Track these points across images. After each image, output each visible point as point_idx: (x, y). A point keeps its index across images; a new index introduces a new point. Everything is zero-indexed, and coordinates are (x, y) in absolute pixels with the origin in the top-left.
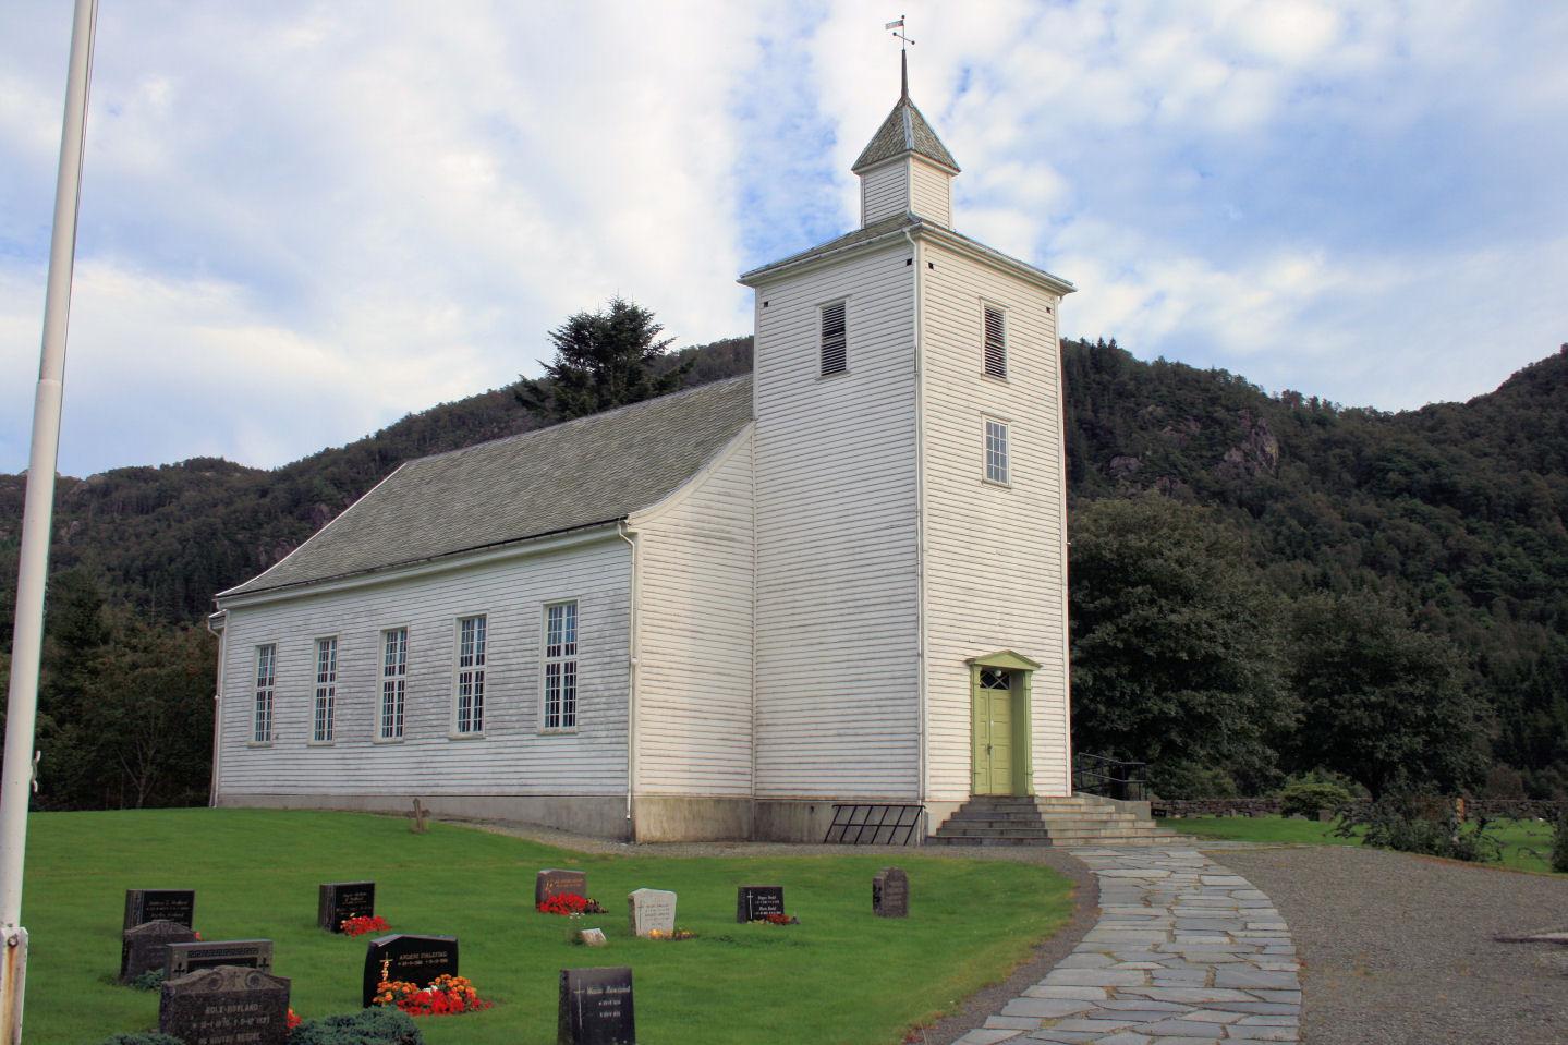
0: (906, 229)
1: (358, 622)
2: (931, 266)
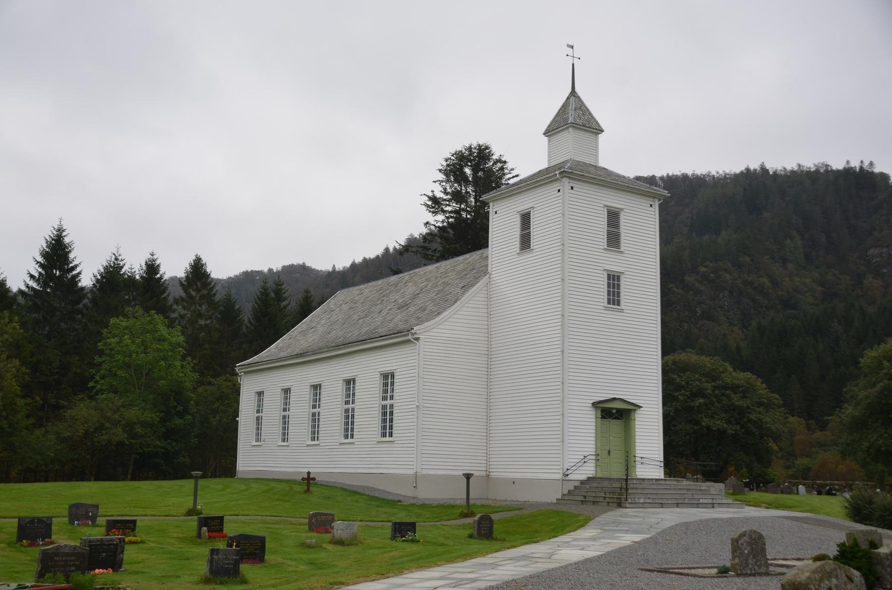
0: (557, 172)
1: (300, 380)
2: (572, 188)
